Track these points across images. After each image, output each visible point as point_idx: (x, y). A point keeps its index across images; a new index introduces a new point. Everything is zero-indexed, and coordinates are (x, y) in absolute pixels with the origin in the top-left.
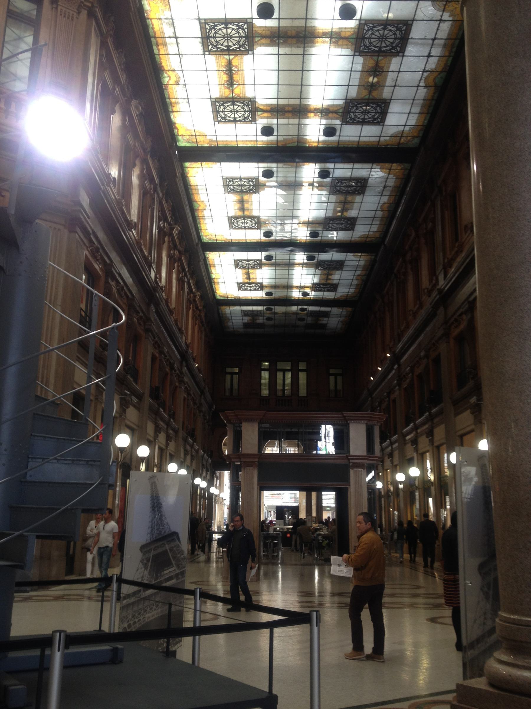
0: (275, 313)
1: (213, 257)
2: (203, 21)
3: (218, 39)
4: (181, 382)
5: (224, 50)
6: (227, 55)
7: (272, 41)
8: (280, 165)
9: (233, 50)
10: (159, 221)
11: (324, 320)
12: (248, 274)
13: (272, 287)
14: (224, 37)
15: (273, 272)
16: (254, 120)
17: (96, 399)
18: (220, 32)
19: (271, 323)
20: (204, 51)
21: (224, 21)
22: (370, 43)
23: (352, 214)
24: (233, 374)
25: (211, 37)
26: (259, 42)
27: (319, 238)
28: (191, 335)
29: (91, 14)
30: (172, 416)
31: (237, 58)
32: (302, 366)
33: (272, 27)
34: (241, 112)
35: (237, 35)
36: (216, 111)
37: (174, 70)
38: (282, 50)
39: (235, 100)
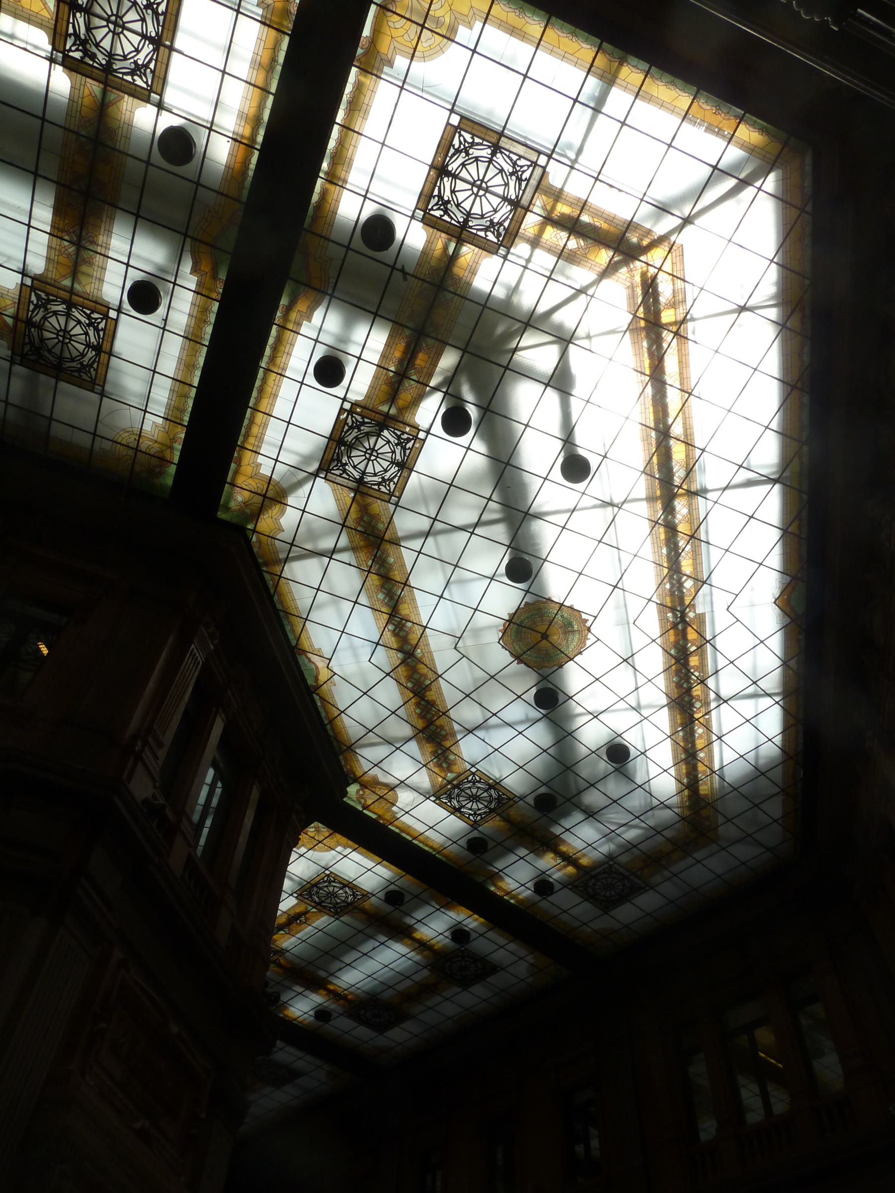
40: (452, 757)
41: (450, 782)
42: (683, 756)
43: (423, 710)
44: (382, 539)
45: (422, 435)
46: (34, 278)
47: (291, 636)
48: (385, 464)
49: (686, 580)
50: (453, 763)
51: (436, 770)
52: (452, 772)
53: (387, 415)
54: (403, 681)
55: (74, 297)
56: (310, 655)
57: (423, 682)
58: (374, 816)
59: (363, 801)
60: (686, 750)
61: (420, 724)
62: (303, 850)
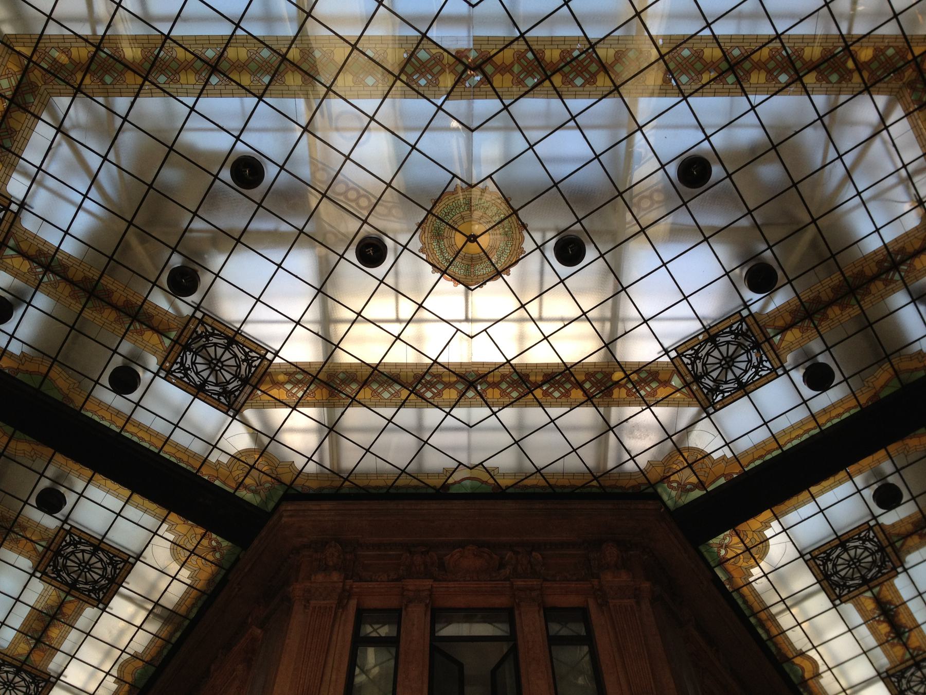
2: (808, 557)
3: (842, 573)
5: (860, 585)
6: (866, 591)
9: (872, 579)
14: (849, 566)
18: (840, 561)
20: (832, 601)
21: (837, 542)
25: (832, 575)
26: (904, 548)
31: (884, 588)
33: (910, 516)
35: (866, 554)
37: (802, 654)
39: (918, 659)
41: (687, 385)
42: (731, 79)
43: (557, 389)
44: (315, 377)
45: (199, 315)
46: (36, 570)
47: (424, 491)
49: (418, 59)
51: (662, 392)
53: (175, 342)
54: (507, 400)
55: (52, 548)
56: (450, 481)
57: (514, 381)
58: (722, 481)
59: (688, 487)
60: (721, 76)
62: (756, 572)
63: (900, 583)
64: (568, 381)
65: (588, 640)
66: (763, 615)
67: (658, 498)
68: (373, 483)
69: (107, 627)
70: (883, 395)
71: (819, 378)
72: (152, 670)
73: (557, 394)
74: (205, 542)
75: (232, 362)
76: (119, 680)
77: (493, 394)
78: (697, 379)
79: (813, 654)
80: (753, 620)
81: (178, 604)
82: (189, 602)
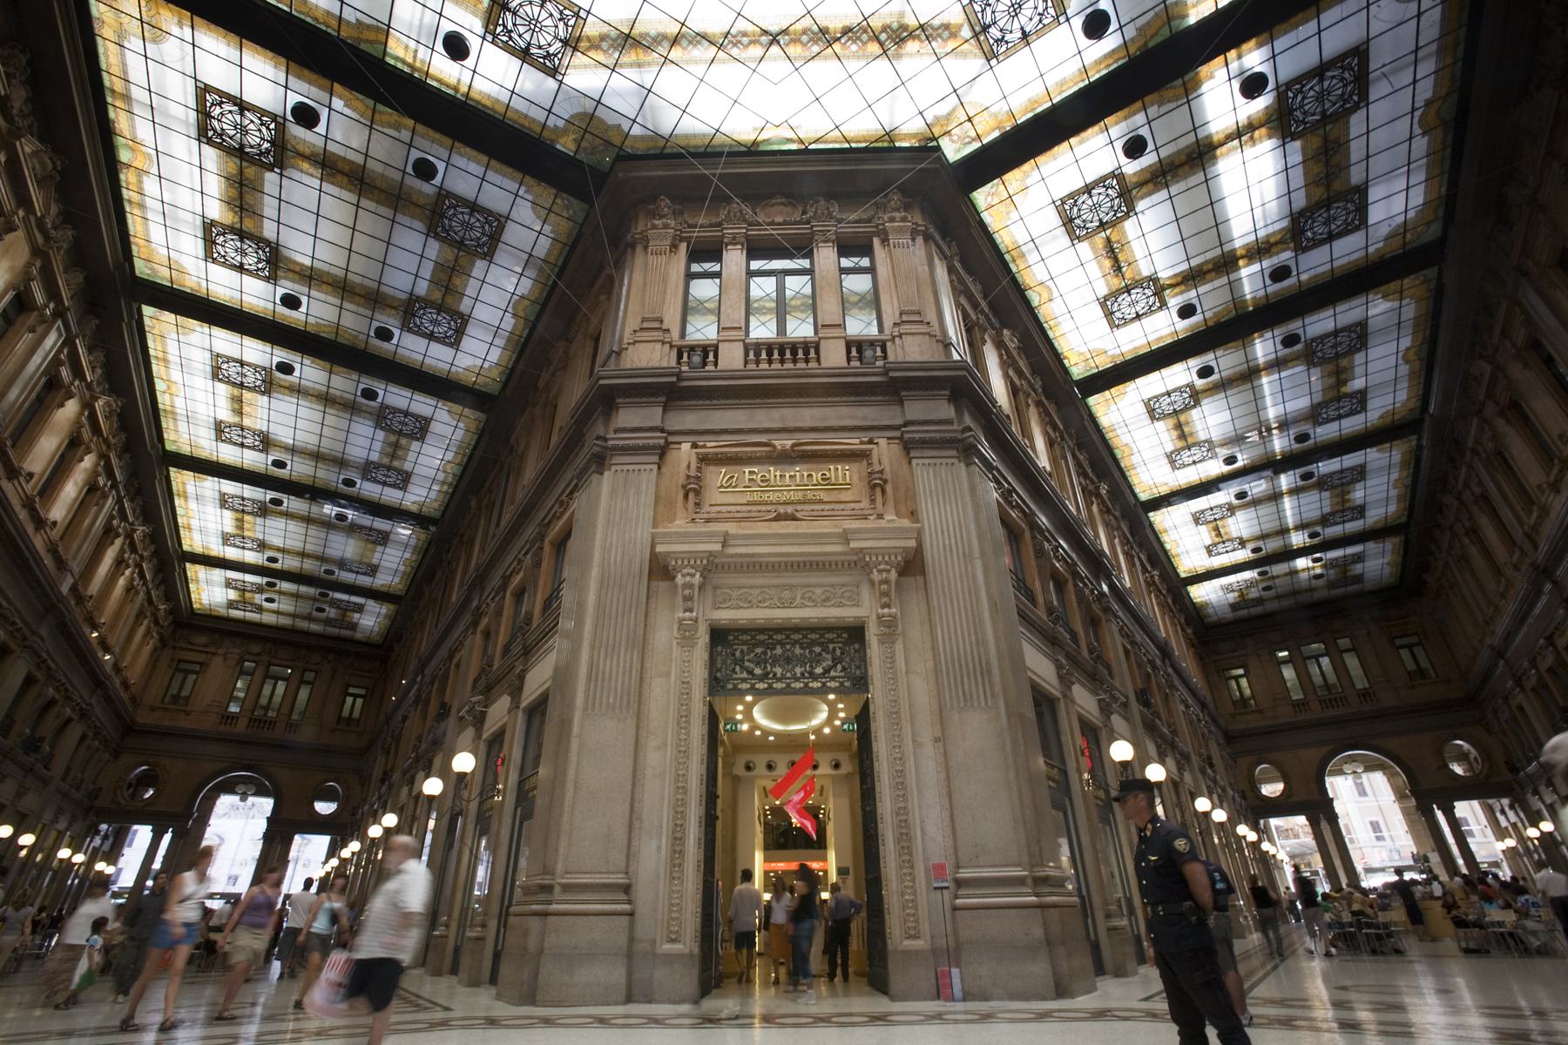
0: (1273, 578)
1: (1161, 519)
4: (1172, 687)
7: (1156, 184)
8: (1219, 353)
10: (1079, 475)
11: (1358, 568)
12: (1217, 529)
13: (1258, 538)
15: (1254, 515)
16: (1164, 304)
17: (1065, 696)
19: (1272, 593)
22: (1305, 113)
23: (1358, 384)
24: (1237, 678)
27: (1311, 442)
28: (1164, 627)
29: (927, 238)
30: (1174, 732)
32: (1344, 643)
34: (1142, 298)
36: (1109, 314)
38: (1174, 189)
40: (936, 23)
41: (976, 35)
48: (544, 15)
50: (946, 27)
51: (951, 44)
52: (962, 25)
54: (808, 54)
58: (996, 134)
61: (874, 48)
63: (1130, 226)
64: (865, 31)
65: (871, 270)
66: (1014, 253)
67: (938, 148)
68: (693, 142)
69: (495, 274)
70: (1151, 45)
71: (1096, 25)
72: (538, 307)
73: (854, 48)
74: (559, 201)
75: (549, 22)
76: (515, 315)
77: (794, 50)
78: (985, 28)
79: (1050, 283)
80: (1007, 257)
81: (548, 254)
82: (556, 253)
